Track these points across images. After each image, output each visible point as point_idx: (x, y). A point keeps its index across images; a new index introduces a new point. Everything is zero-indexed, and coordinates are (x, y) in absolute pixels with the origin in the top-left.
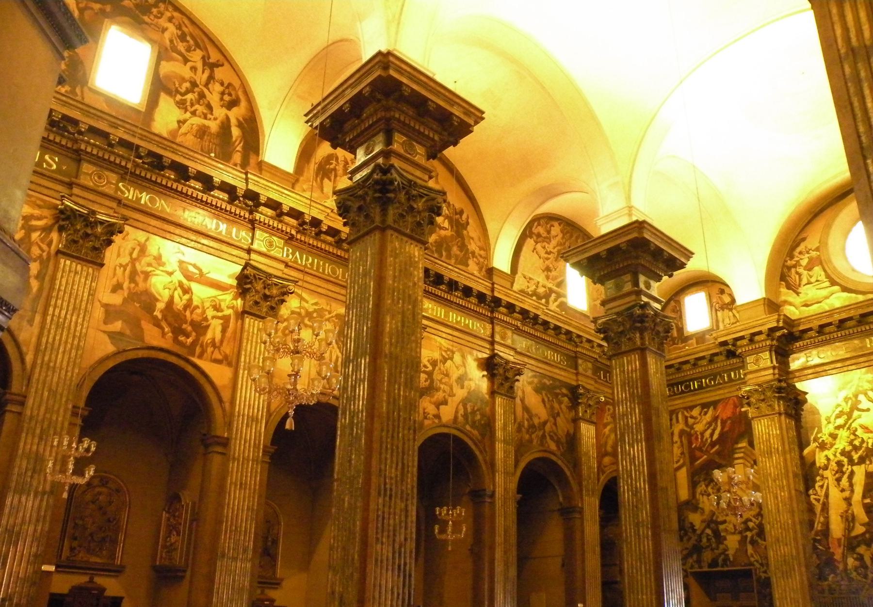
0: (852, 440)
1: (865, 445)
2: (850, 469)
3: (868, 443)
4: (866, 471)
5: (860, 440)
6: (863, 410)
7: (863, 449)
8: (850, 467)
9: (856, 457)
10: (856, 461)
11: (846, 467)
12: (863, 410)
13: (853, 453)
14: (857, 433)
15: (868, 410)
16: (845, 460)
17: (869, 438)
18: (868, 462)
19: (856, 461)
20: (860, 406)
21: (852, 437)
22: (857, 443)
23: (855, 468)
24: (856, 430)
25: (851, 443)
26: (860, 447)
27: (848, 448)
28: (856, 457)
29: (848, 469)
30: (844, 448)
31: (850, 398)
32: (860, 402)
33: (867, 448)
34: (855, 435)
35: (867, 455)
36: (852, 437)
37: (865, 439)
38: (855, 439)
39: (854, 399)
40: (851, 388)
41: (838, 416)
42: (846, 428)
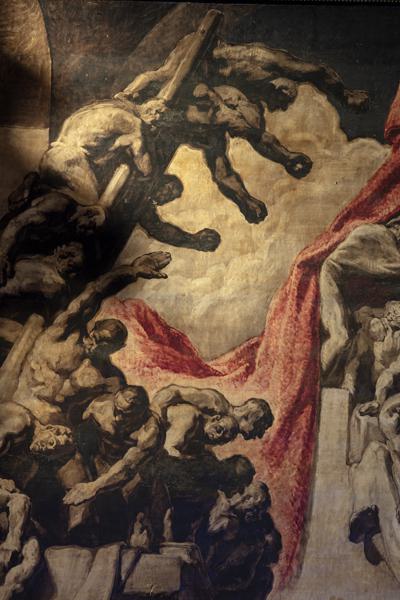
0: (84, 396)
1: (144, 435)
2: (28, 563)
3: (164, 426)
4: (118, 584)
5: (124, 400)
6: (180, 238)
7: (131, 454)
8: (32, 545)
9: (80, 492)
10: (76, 519)
11: (11, 543)
12: (180, 238)
13: (70, 471)
14: (115, 358)
15: (208, 241)
16: (18, 502)
17: (177, 400)
18: (139, 538)
19: (76, 519)
20: (169, 213)
21: (86, 376)
22: (104, 413)
23: (62, 561)
24: (119, 338)
25: (72, 407)
26: (121, 439)
27: (49, 437)
28: (80, 492)
29: (17, 558)
30: (28, 431)
31: (125, 156)
32: (176, 187)
33: (156, 450)
34: (107, 369)
35: (142, 491)
36: (86, 376)
37: (156, 397)
38: (100, 392)
39: (144, 164)
40: (147, 93)
41: (34, 243)
42: (61, 317)
